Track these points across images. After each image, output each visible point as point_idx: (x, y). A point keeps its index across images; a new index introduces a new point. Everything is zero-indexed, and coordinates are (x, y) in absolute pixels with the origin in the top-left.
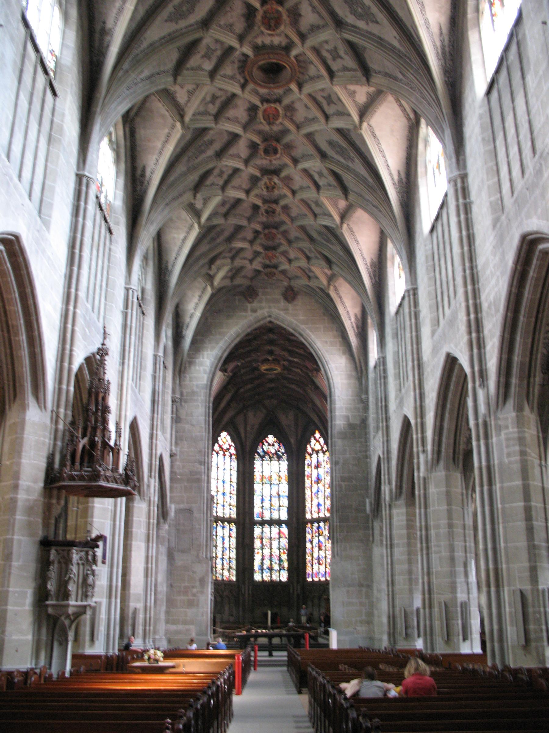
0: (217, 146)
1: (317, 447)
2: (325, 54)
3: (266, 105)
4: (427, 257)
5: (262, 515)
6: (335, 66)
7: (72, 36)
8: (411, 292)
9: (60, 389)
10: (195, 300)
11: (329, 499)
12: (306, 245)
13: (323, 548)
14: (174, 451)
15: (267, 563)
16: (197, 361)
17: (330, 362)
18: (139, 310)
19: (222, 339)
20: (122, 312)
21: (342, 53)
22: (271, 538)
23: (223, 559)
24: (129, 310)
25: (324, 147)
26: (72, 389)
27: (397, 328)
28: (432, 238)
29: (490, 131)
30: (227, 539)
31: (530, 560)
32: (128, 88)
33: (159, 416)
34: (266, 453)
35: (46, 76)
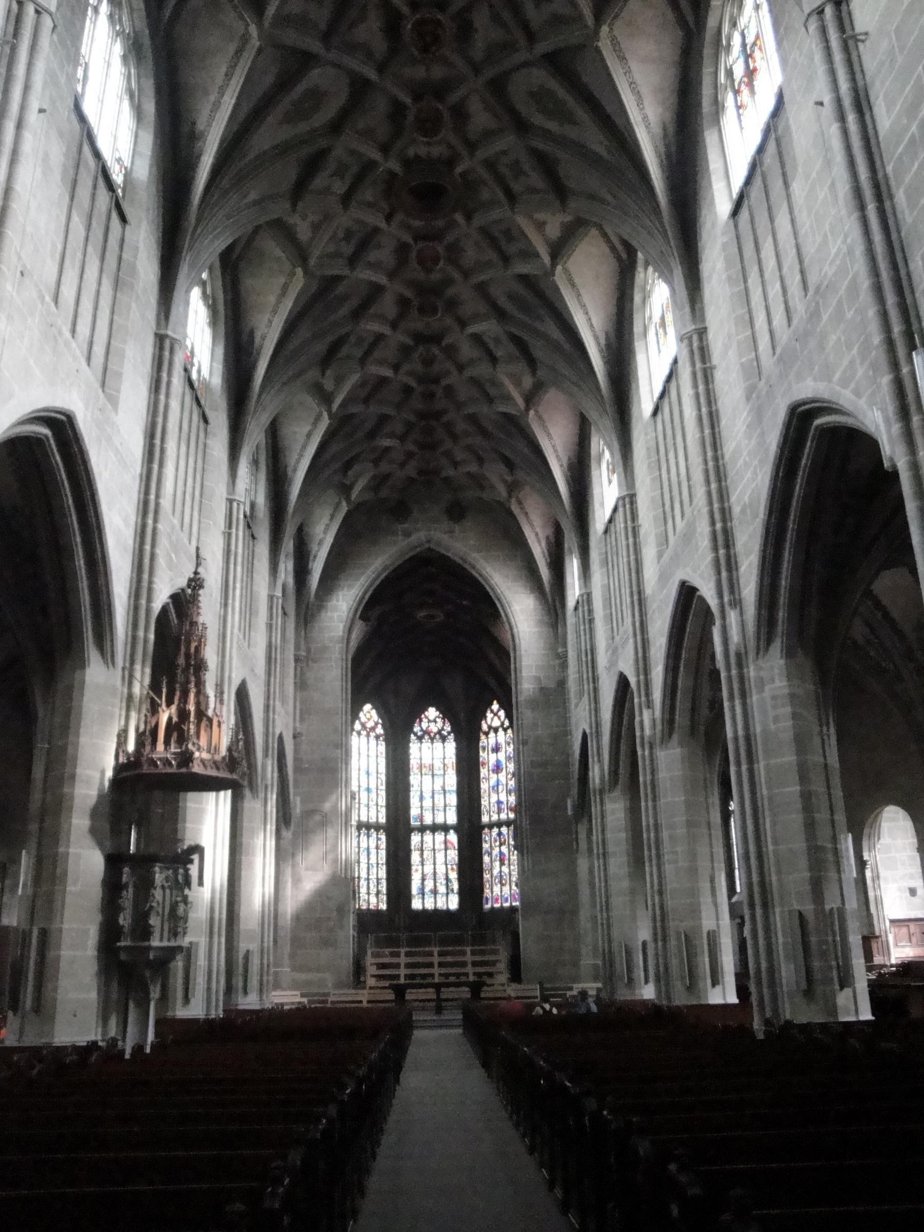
0: (354, 302)
1: (496, 723)
2: (504, 170)
3: (421, 244)
4: (648, 449)
5: (421, 817)
6: (516, 187)
7: (148, 139)
8: (627, 500)
9: (134, 638)
10: (325, 520)
11: (513, 794)
12: (477, 441)
13: (506, 862)
14: (298, 730)
15: (429, 885)
16: (329, 604)
17: (514, 604)
18: (247, 533)
19: (363, 574)
20: (224, 533)
21: (526, 168)
23: (368, 879)
24: (234, 530)
25: (503, 302)
26: (152, 637)
27: (606, 553)
28: (655, 422)
29: (739, 266)
30: (373, 851)
31: (811, 869)
32: (228, 217)
33: (278, 680)
34: (426, 732)
35: (111, 193)
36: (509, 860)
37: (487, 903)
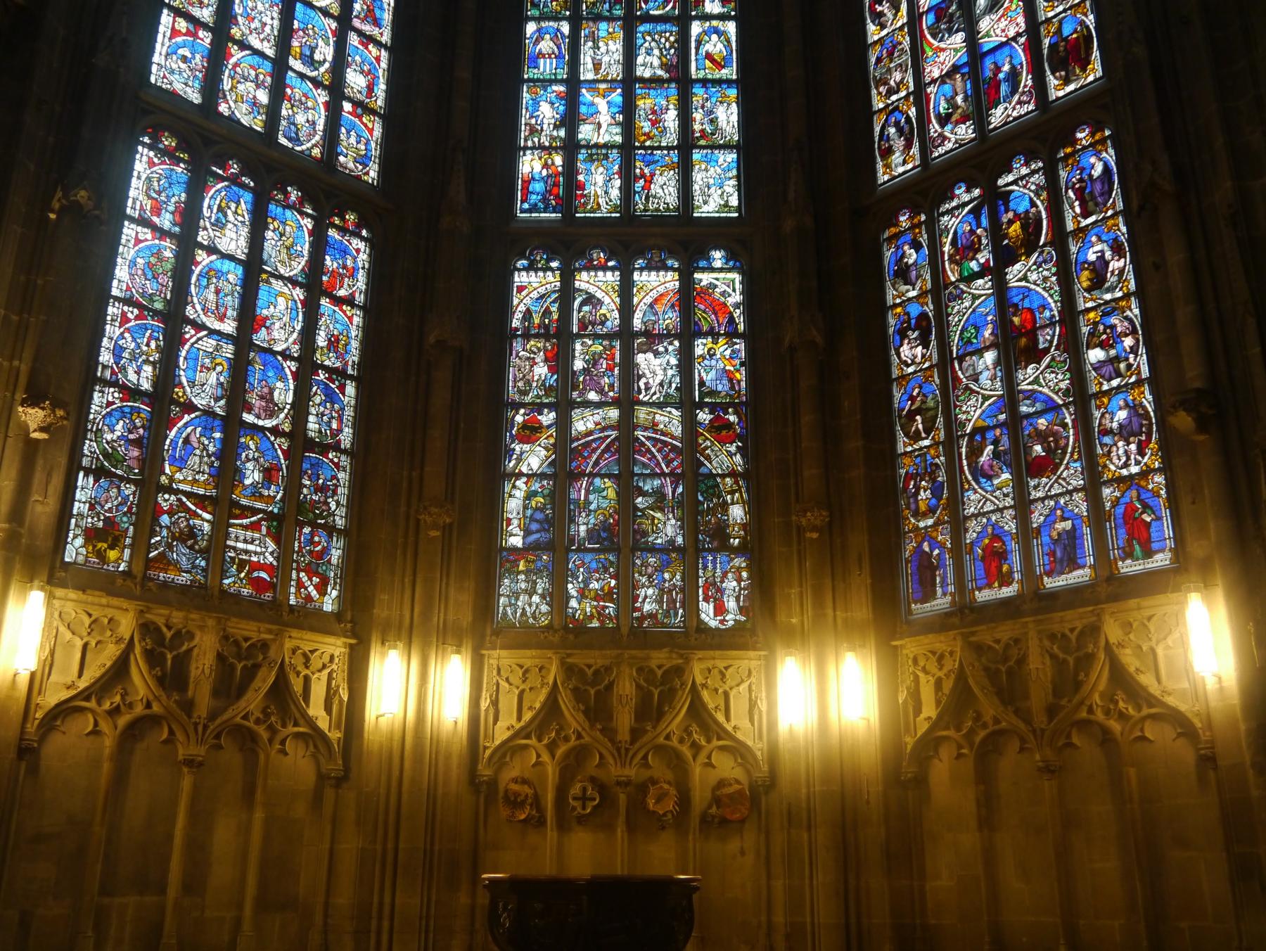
22: (625, 333)
23: (232, 425)
36: (1069, 313)
37: (929, 595)
